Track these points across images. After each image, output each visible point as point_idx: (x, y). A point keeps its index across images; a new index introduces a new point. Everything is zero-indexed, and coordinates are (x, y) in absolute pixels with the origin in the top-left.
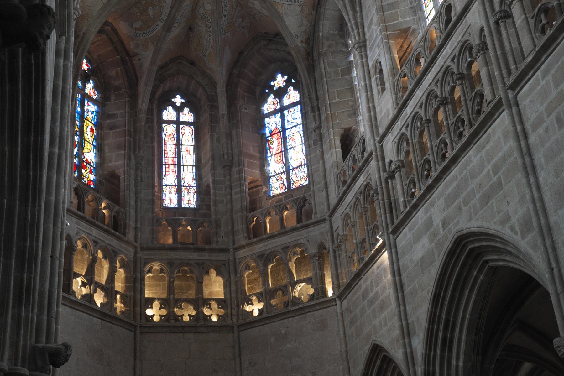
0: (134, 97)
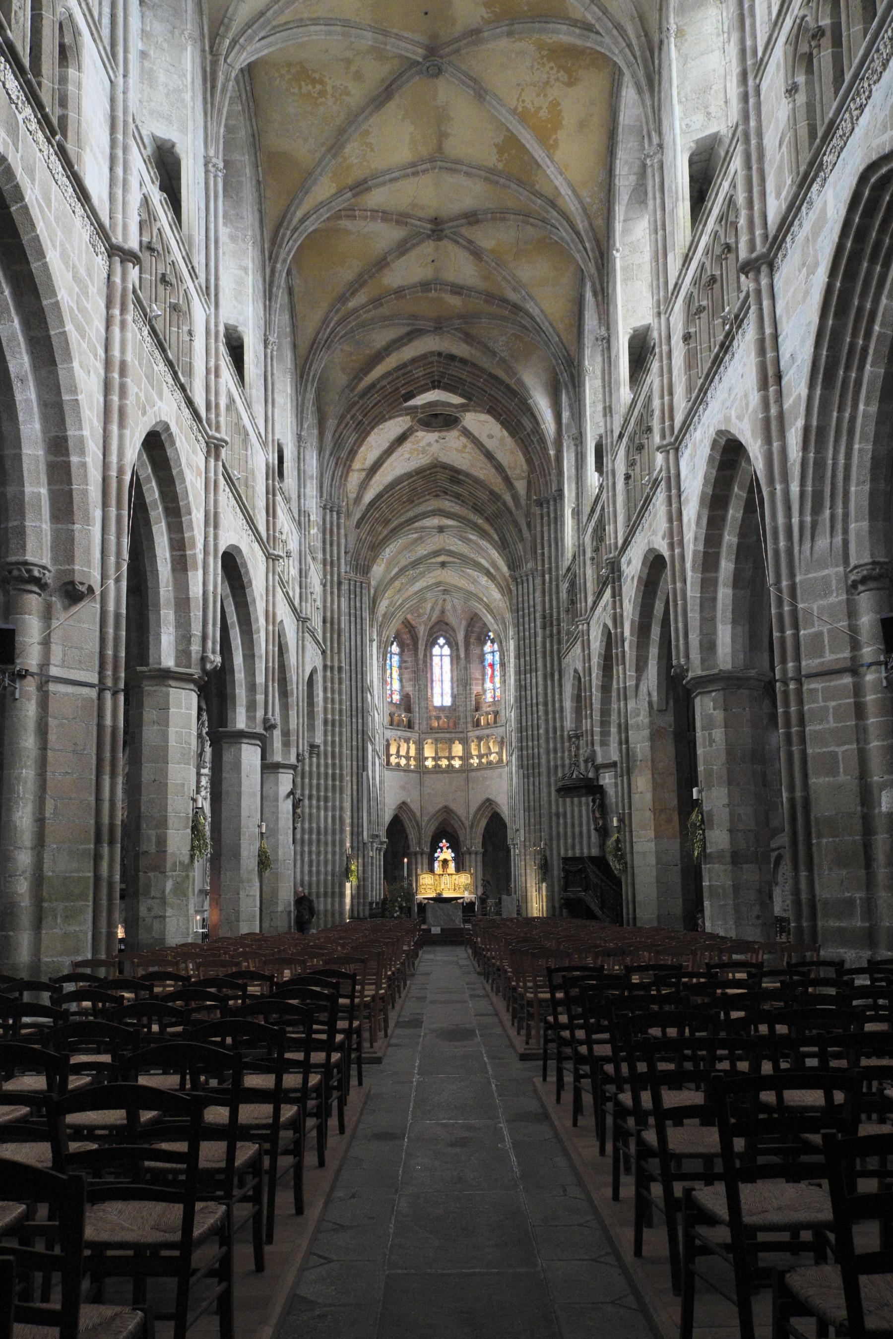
0: (416, 649)
